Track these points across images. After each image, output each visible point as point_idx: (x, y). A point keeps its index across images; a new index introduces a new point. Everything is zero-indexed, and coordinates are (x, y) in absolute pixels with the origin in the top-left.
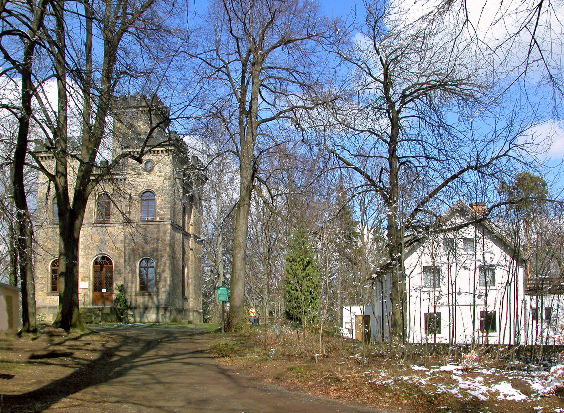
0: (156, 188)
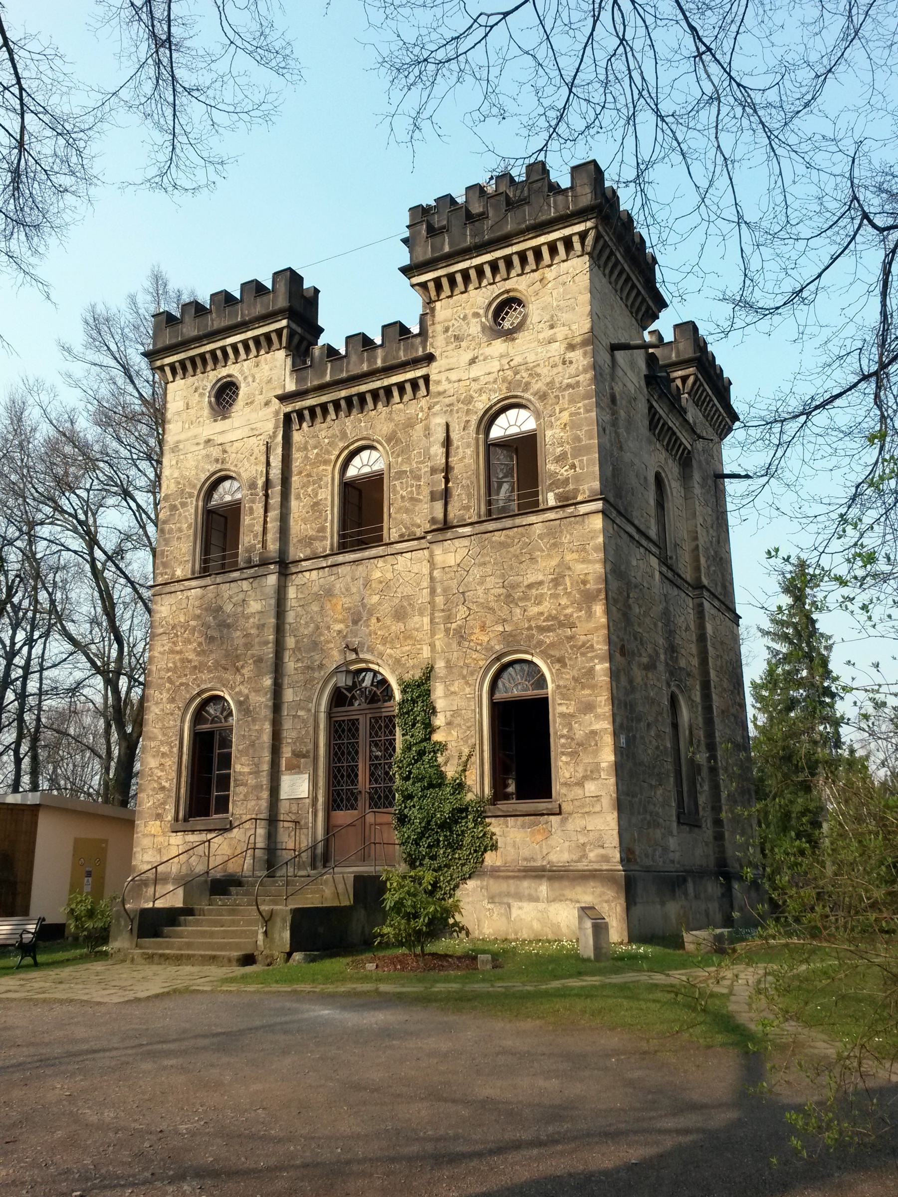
0: (538, 386)
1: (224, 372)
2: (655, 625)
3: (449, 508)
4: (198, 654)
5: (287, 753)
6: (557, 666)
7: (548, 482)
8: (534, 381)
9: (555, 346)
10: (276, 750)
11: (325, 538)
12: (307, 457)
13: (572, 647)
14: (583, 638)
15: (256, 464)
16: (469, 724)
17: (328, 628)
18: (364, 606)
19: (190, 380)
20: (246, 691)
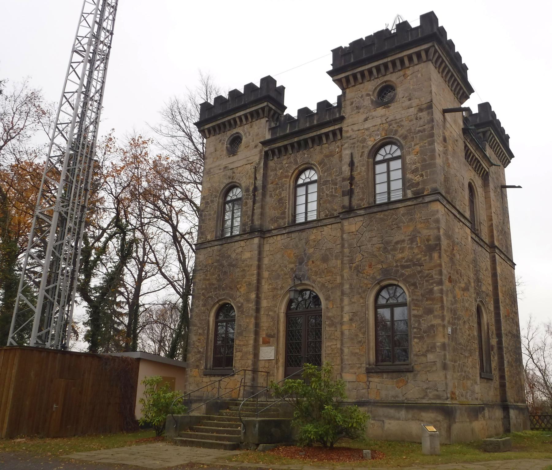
0: (402, 131)
1: (235, 131)
2: (469, 266)
3: (353, 200)
4: (218, 281)
5: (263, 334)
6: (412, 288)
7: (408, 184)
8: (400, 129)
9: (411, 110)
10: (257, 333)
11: (285, 218)
12: (276, 174)
13: (420, 277)
14: (427, 272)
15: (250, 179)
16: (362, 320)
17: (286, 267)
18: (305, 254)
19: (218, 136)
20: (242, 301)
